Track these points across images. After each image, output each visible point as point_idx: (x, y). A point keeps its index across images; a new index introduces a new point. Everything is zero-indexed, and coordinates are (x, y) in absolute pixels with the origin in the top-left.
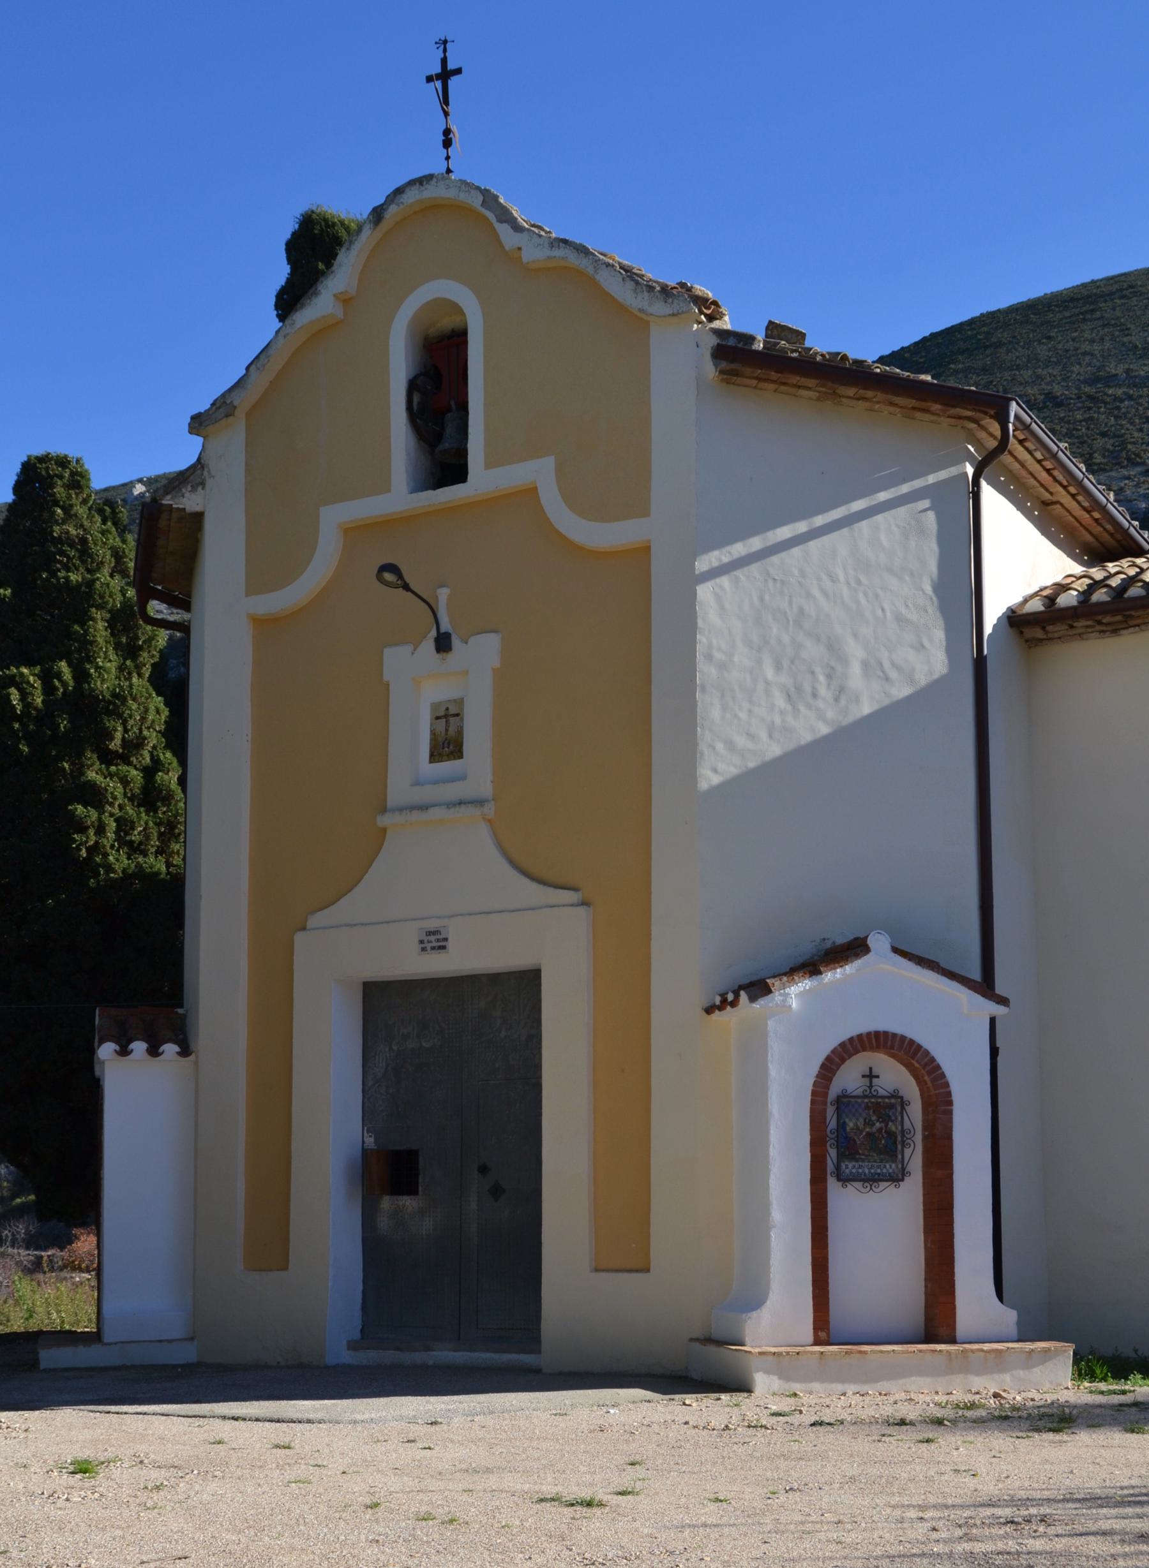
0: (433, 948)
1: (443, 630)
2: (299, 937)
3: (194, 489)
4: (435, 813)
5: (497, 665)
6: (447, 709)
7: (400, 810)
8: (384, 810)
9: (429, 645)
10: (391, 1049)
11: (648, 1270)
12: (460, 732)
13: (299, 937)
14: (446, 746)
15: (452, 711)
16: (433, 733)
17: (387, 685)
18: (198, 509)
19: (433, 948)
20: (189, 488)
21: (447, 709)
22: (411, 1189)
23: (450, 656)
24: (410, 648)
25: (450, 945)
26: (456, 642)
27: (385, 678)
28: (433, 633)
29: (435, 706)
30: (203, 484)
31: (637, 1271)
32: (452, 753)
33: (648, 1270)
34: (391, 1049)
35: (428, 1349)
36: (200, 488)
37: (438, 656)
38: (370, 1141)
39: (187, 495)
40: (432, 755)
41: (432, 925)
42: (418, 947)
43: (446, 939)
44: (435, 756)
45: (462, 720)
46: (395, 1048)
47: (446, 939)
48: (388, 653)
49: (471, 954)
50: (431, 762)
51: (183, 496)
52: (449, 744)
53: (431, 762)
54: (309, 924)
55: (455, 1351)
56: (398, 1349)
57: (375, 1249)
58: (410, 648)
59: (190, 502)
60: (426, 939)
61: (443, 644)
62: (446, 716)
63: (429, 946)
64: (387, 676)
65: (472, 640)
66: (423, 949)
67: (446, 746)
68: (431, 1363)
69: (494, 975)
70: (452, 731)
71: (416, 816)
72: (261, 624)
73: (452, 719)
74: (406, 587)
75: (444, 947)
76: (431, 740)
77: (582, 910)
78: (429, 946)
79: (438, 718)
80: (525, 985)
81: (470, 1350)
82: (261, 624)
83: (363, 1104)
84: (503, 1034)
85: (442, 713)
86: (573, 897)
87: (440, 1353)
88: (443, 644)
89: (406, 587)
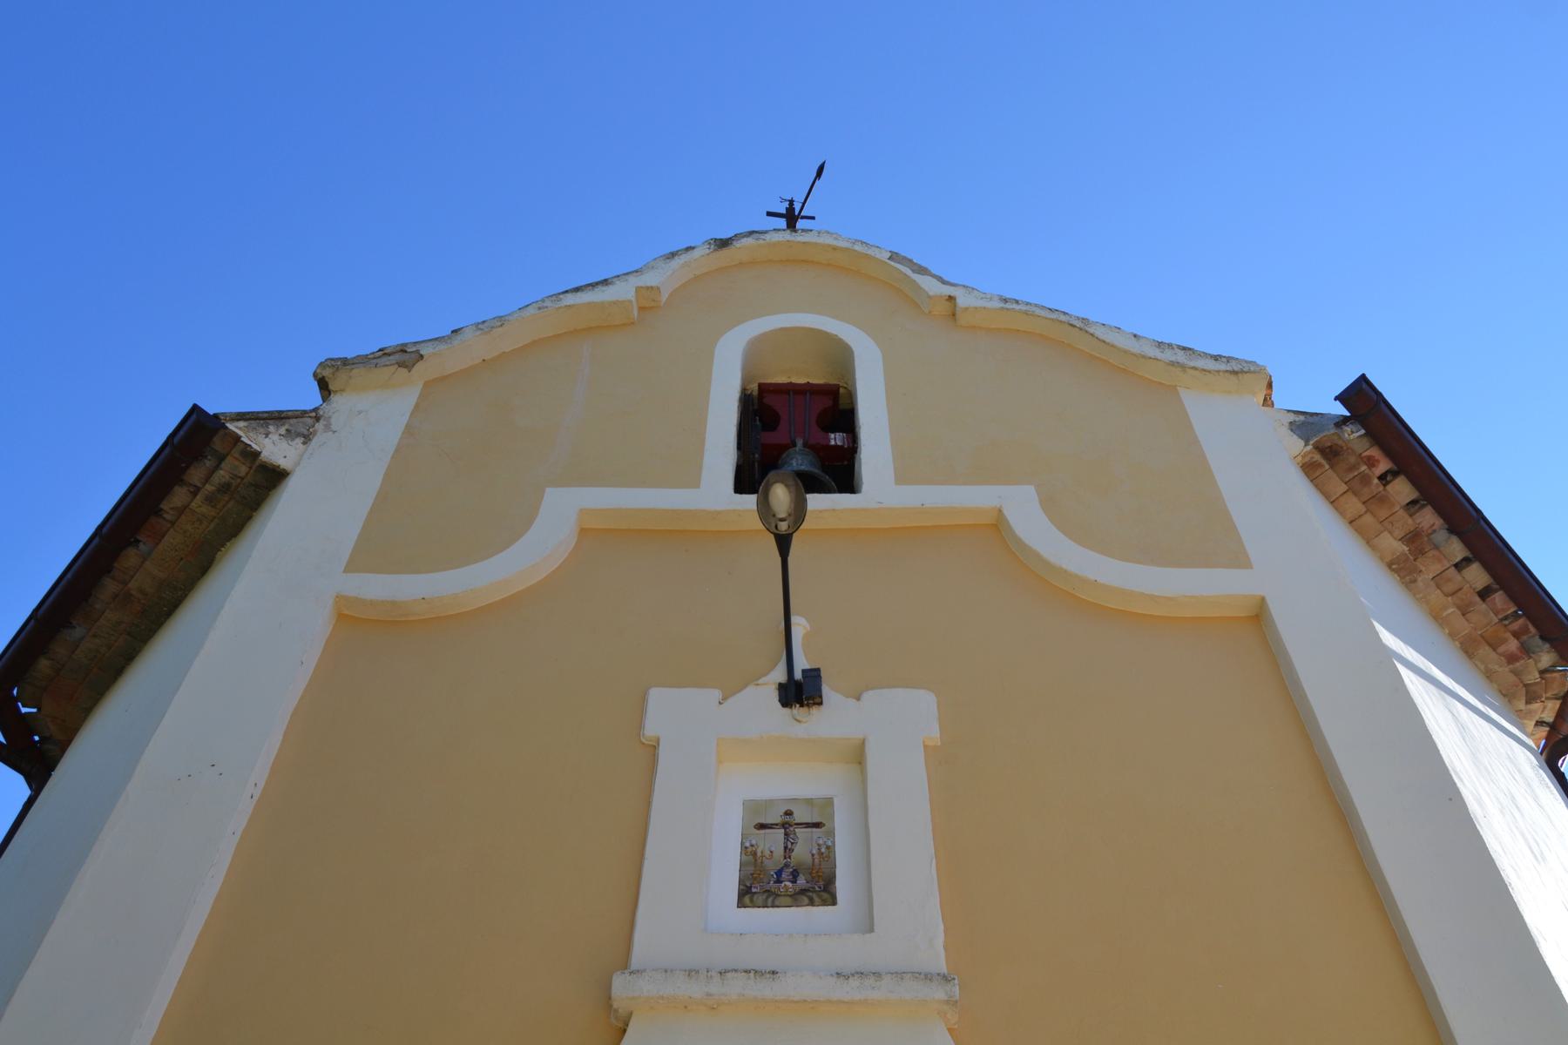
1: (798, 675)
3: (290, 435)
5: (934, 734)
6: (789, 813)
12: (827, 855)
14: (790, 869)
15: (801, 815)
16: (750, 856)
17: (653, 748)
18: (284, 463)
20: (283, 430)
21: (789, 813)
24: (716, 694)
27: (651, 729)
28: (780, 675)
29: (751, 807)
30: (307, 438)
32: (803, 892)
36: (299, 440)
37: (787, 710)
39: (275, 437)
40: (741, 895)
45: (831, 834)
48: (656, 696)
50: (741, 904)
51: (267, 435)
52: (794, 876)
53: (741, 904)
58: (716, 694)
59: (274, 448)
62: (785, 825)
65: (867, 696)
67: (790, 869)
74: (784, 543)
79: (762, 826)
85: (775, 817)
88: (800, 692)
89: (784, 543)
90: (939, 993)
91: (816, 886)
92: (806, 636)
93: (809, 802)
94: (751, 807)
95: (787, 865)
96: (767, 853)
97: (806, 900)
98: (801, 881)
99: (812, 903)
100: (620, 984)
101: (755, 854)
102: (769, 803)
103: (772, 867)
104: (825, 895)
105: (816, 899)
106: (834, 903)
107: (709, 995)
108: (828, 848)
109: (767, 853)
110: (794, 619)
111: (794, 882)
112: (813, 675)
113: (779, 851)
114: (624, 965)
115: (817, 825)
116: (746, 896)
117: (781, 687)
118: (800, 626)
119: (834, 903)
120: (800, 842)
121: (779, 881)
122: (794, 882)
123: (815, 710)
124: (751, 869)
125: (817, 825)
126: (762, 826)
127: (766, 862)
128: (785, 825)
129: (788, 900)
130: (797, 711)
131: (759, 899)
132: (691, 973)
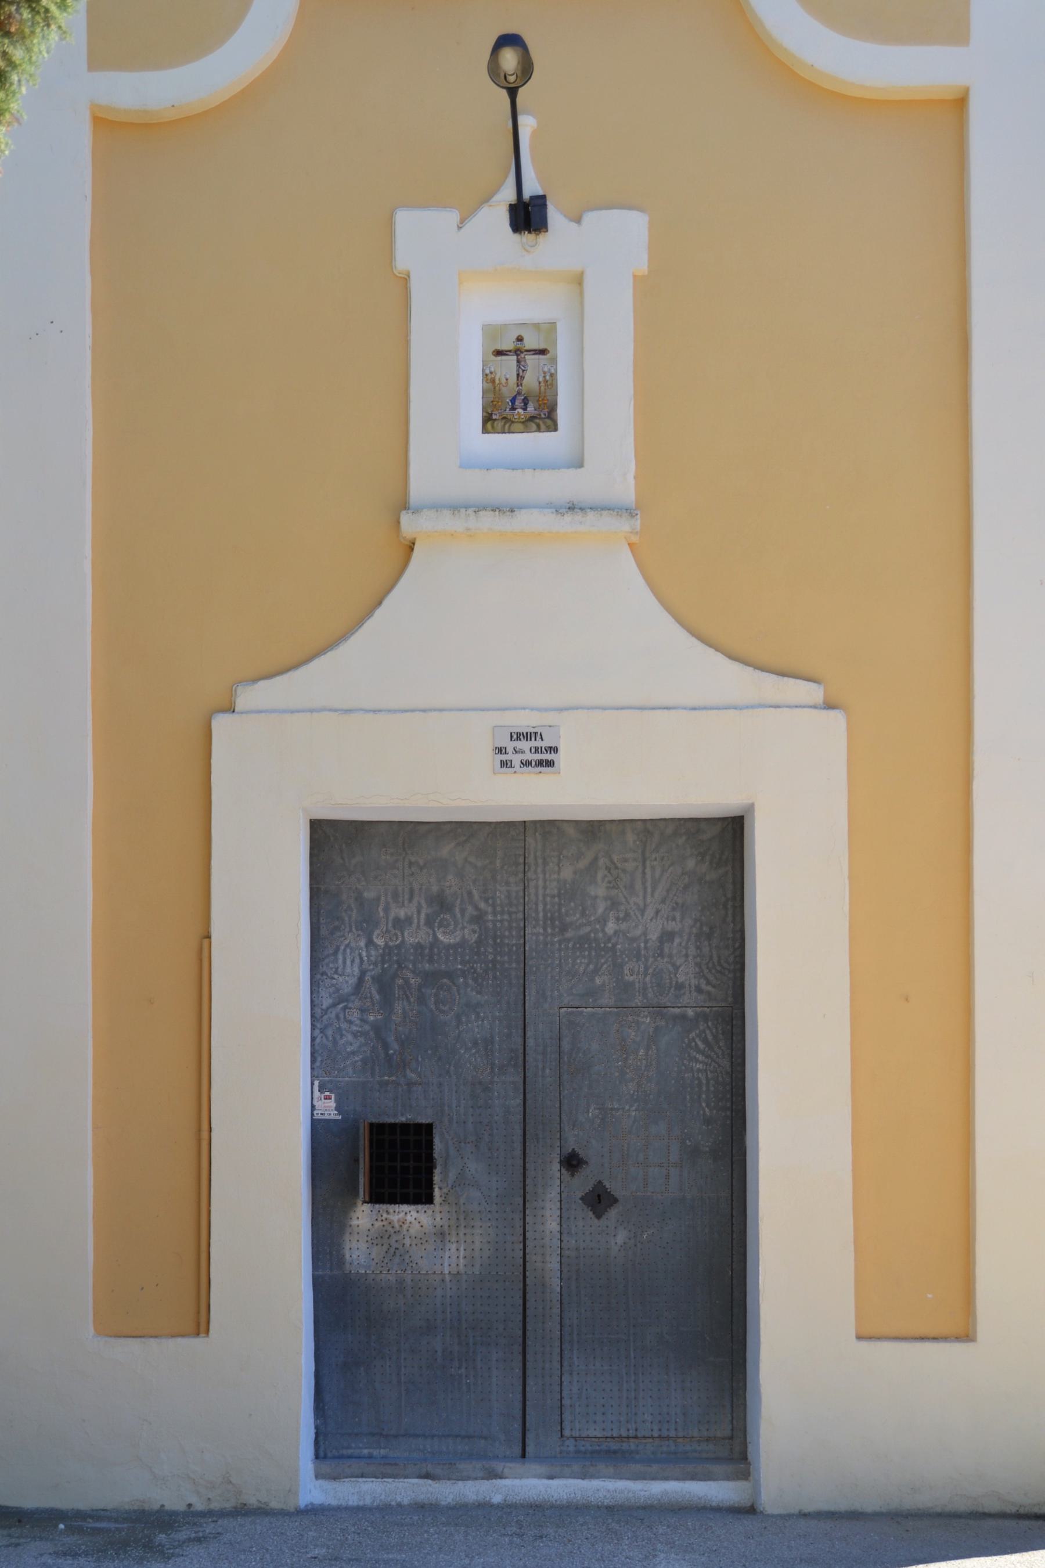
0: (527, 764)
1: (527, 195)
2: (221, 724)
4: (524, 521)
6: (520, 339)
7: (437, 507)
8: (405, 506)
9: (496, 215)
10: (370, 943)
11: (967, 1336)
12: (550, 382)
13: (221, 724)
15: (530, 343)
19: (527, 764)
21: (520, 339)
22: (423, 1196)
23: (543, 240)
24: (454, 216)
25: (561, 759)
26: (554, 215)
28: (508, 194)
29: (491, 331)
31: (922, 1339)
32: (532, 418)
33: (967, 1336)
34: (370, 943)
35: (493, 1475)
38: (328, 1108)
41: (525, 722)
42: (488, 759)
43: (554, 750)
44: (494, 419)
45: (554, 361)
46: (380, 942)
47: (554, 750)
49: (601, 780)
50: (485, 431)
52: (526, 402)
53: (485, 431)
54: (241, 704)
55: (551, 1477)
56: (427, 1476)
57: (343, 1306)
58: (454, 216)
60: (510, 746)
61: (528, 216)
62: (517, 352)
63: (516, 759)
64: (403, 261)
65: (590, 218)
66: (504, 764)
68: (497, 1499)
69: (591, 823)
70: (531, 380)
71: (488, 521)
72: (108, 126)
73: (531, 359)
75: (550, 764)
76: (485, 392)
77: (837, 720)
78: (516, 759)
79: (499, 353)
80: (725, 840)
81: (584, 1476)
82: (108, 126)
83: (313, 1039)
84: (611, 927)
85: (508, 344)
86: (813, 693)
87: (517, 1482)
88: (528, 216)
90: (624, 526)
91: (541, 413)
92: (535, 134)
93: (537, 326)
94: (491, 331)
95: (519, 393)
96: (503, 381)
97: (534, 427)
98: (531, 408)
99: (539, 430)
100: (405, 518)
101: (493, 381)
102: (504, 327)
103: (508, 392)
104: (549, 422)
105: (543, 426)
106: (556, 430)
107: (468, 529)
108: (552, 375)
109: (503, 381)
110: (522, 120)
111: (525, 409)
112: (540, 201)
113: (513, 379)
114: (405, 506)
115: (543, 352)
116: (489, 422)
117: (513, 209)
118: (527, 124)
119: (556, 430)
120: (529, 369)
121: (513, 409)
122: (525, 409)
123: (542, 238)
124: (491, 396)
125: (543, 352)
126: (499, 353)
127: (504, 390)
128: (517, 352)
129: (520, 426)
130: (527, 237)
131: (499, 425)
132: (455, 508)
